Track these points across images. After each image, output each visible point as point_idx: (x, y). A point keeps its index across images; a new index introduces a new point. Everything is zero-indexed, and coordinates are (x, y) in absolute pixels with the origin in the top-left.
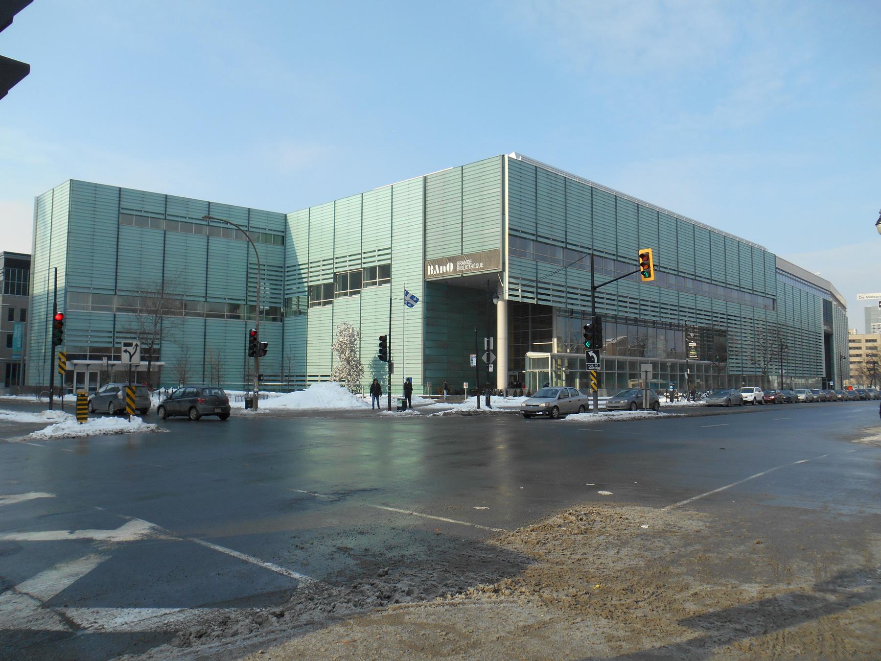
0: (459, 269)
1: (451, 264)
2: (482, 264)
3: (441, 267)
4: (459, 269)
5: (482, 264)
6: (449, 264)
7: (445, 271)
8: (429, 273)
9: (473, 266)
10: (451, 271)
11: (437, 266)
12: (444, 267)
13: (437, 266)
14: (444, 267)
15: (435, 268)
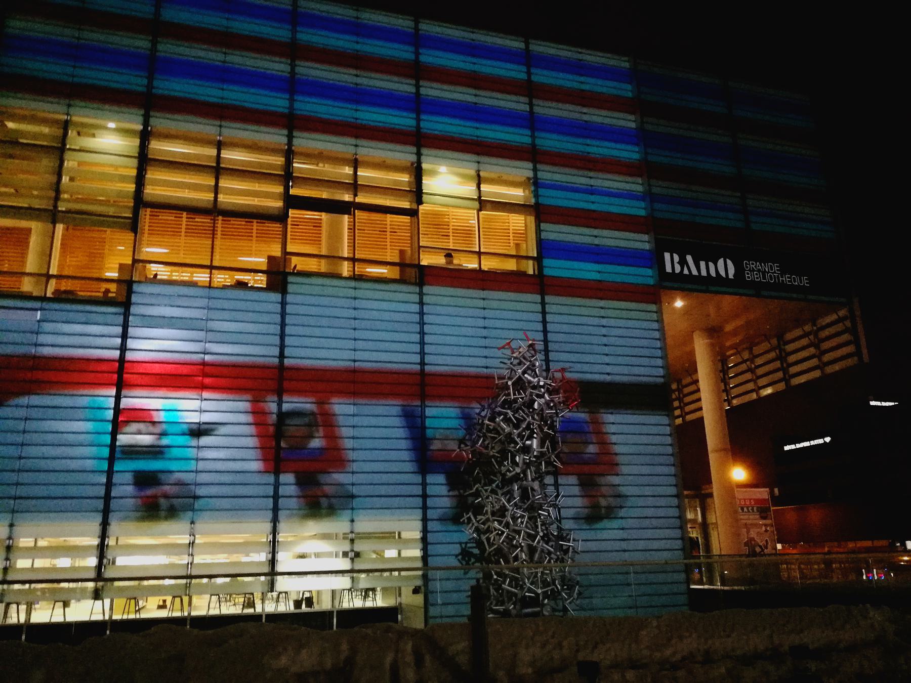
0: (748, 276)
1: (729, 262)
2: (805, 281)
3: (703, 264)
4: (748, 276)
5: (805, 281)
6: (721, 262)
7: (713, 274)
8: (669, 269)
9: (786, 279)
10: (731, 276)
11: (689, 258)
12: (711, 265)
13: (689, 258)
14: (711, 265)
15: (683, 262)
